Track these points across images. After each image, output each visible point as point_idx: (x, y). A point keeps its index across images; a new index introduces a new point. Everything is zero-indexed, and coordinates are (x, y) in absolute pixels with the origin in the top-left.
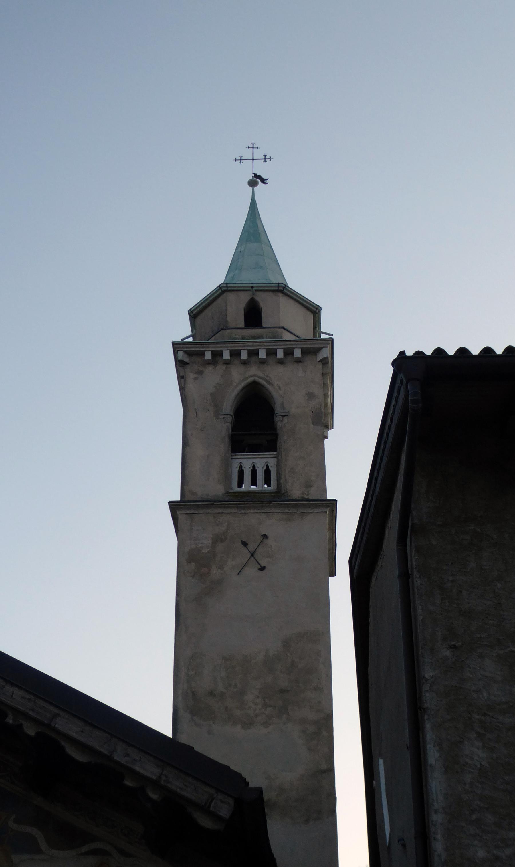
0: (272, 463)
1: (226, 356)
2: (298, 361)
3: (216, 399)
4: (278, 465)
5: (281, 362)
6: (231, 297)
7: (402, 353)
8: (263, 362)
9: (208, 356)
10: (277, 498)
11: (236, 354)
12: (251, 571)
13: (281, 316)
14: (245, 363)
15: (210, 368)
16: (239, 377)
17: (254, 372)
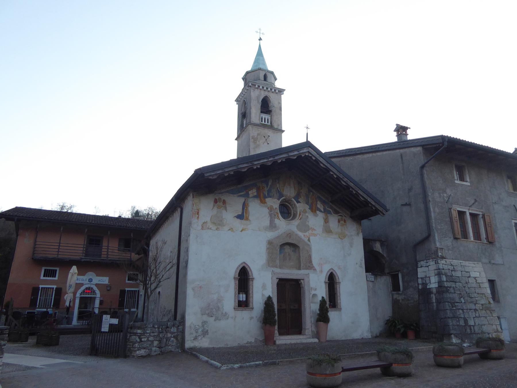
0: (269, 118)
1: (261, 87)
2: (277, 93)
3: (258, 98)
4: (271, 119)
5: (273, 92)
6: (261, 71)
7: (401, 130)
8: (269, 91)
9: (257, 86)
10: (271, 127)
11: (263, 87)
12: (266, 144)
13: (270, 78)
14: (265, 90)
16: (263, 94)
17: (266, 94)
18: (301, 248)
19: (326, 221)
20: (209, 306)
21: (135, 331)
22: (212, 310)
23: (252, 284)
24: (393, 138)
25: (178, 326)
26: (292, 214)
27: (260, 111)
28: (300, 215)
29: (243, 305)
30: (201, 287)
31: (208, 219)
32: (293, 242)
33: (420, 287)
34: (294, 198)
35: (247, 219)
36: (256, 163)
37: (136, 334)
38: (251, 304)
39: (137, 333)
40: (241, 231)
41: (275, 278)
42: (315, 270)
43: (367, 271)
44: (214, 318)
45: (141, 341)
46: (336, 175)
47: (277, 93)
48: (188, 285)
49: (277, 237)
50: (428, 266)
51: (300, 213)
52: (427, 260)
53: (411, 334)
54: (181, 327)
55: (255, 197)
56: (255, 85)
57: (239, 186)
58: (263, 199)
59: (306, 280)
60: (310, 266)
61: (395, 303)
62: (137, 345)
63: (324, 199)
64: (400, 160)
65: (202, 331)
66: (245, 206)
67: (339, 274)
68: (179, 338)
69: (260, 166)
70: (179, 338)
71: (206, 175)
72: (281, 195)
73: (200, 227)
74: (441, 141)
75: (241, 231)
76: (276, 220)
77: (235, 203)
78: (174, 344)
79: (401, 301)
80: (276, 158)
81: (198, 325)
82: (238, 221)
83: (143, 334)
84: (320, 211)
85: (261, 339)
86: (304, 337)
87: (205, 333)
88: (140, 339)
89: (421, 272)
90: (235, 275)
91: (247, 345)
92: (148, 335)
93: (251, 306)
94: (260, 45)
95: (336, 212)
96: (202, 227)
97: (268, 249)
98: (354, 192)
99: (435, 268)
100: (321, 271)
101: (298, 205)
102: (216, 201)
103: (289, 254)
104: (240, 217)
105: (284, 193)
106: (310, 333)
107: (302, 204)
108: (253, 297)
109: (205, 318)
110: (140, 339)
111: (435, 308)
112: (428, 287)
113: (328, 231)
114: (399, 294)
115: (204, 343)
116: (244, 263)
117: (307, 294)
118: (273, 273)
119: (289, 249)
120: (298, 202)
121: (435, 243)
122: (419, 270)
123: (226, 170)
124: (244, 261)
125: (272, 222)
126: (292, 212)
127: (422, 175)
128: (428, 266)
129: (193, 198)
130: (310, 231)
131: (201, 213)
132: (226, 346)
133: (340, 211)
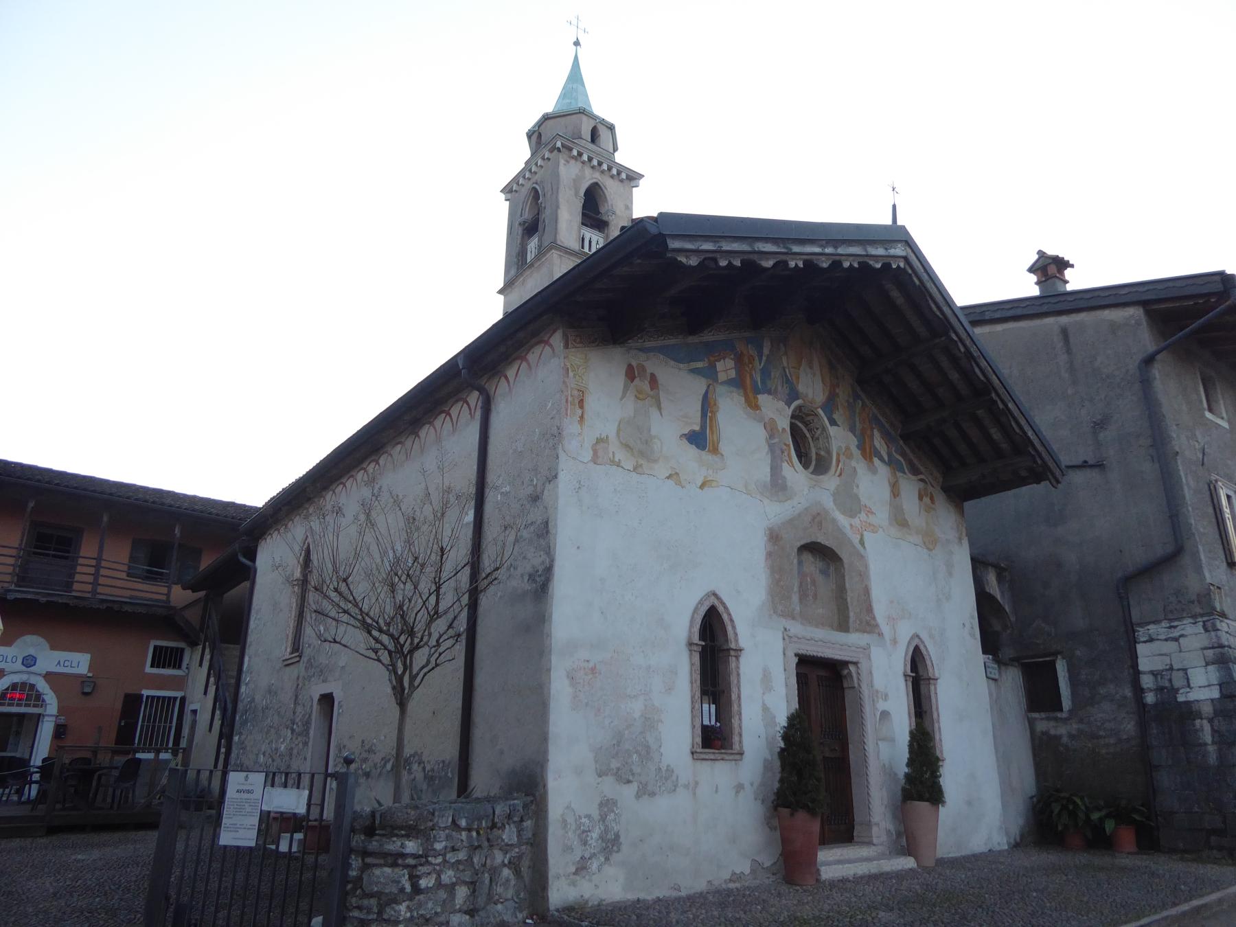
2: (622, 181)
3: (576, 182)
5: (612, 177)
6: (584, 118)
8: (603, 172)
9: (575, 153)
11: (590, 159)
14: (593, 167)
15: (573, 162)
16: (590, 177)
17: (597, 177)
18: (845, 561)
19: (895, 492)
20: (619, 743)
21: (393, 846)
22: (626, 761)
23: (738, 668)
24: (1029, 288)
25: (522, 820)
26: (814, 457)
27: (579, 218)
28: (838, 461)
29: (715, 739)
30: (593, 670)
31: (610, 430)
32: (826, 543)
33: (1150, 698)
34: (823, 407)
35: (715, 450)
36: (796, 249)
37: (395, 859)
38: (736, 739)
39: (403, 856)
40: (702, 487)
41: (791, 654)
42: (881, 634)
43: (984, 653)
44: (634, 787)
45: (417, 890)
46: (964, 345)
47: (622, 181)
48: (555, 660)
49: (791, 522)
50: (1176, 639)
51: (838, 455)
52: (1171, 620)
53: (1127, 837)
54: (528, 824)
55: (730, 382)
56: (570, 149)
57: (692, 339)
58: (751, 395)
59: (863, 666)
60: (870, 626)
61: (1045, 751)
62: (403, 907)
63: (887, 426)
64: (1060, 345)
65: (601, 838)
66: (707, 407)
67: (932, 651)
68: (525, 865)
69: (805, 262)
70: (525, 865)
71: (674, 244)
72: (793, 395)
73: (587, 455)
74: (1220, 287)
75: (702, 487)
76: (785, 465)
77: (682, 390)
78: (510, 893)
79: (1065, 740)
80: (840, 251)
81: (588, 816)
82: (692, 451)
83: (422, 858)
84: (881, 459)
85: (767, 864)
86: (864, 852)
87: (611, 844)
88: (414, 879)
89: (1149, 657)
90: (690, 638)
91: (732, 886)
92: (440, 860)
93: (736, 747)
94: (576, 57)
95: (915, 471)
96: (595, 452)
97: (769, 555)
98: (1001, 406)
99: (1206, 643)
100: (895, 641)
101: (832, 430)
102: (631, 374)
103: (814, 582)
104: (698, 439)
105: (801, 388)
106: (884, 838)
107: (840, 429)
108: (740, 714)
109: (609, 787)
110: (414, 879)
111: (1213, 759)
112: (1181, 698)
113: (900, 521)
114: (1056, 719)
115: (609, 886)
116: (715, 594)
117: (867, 709)
118: (787, 637)
119: (817, 563)
120: (833, 423)
121: (1199, 569)
122: (1141, 649)
123: (727, 246)
124: (712, 587)
125: (775, 470)
126: (813, 451)
127: (1146, 383)
128: (1176, 639)
129: (566, 346)
130: (863, 516)
131: (592, 403)
132: (675, 894)
133: (922, 469)
